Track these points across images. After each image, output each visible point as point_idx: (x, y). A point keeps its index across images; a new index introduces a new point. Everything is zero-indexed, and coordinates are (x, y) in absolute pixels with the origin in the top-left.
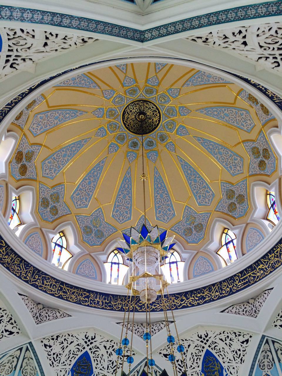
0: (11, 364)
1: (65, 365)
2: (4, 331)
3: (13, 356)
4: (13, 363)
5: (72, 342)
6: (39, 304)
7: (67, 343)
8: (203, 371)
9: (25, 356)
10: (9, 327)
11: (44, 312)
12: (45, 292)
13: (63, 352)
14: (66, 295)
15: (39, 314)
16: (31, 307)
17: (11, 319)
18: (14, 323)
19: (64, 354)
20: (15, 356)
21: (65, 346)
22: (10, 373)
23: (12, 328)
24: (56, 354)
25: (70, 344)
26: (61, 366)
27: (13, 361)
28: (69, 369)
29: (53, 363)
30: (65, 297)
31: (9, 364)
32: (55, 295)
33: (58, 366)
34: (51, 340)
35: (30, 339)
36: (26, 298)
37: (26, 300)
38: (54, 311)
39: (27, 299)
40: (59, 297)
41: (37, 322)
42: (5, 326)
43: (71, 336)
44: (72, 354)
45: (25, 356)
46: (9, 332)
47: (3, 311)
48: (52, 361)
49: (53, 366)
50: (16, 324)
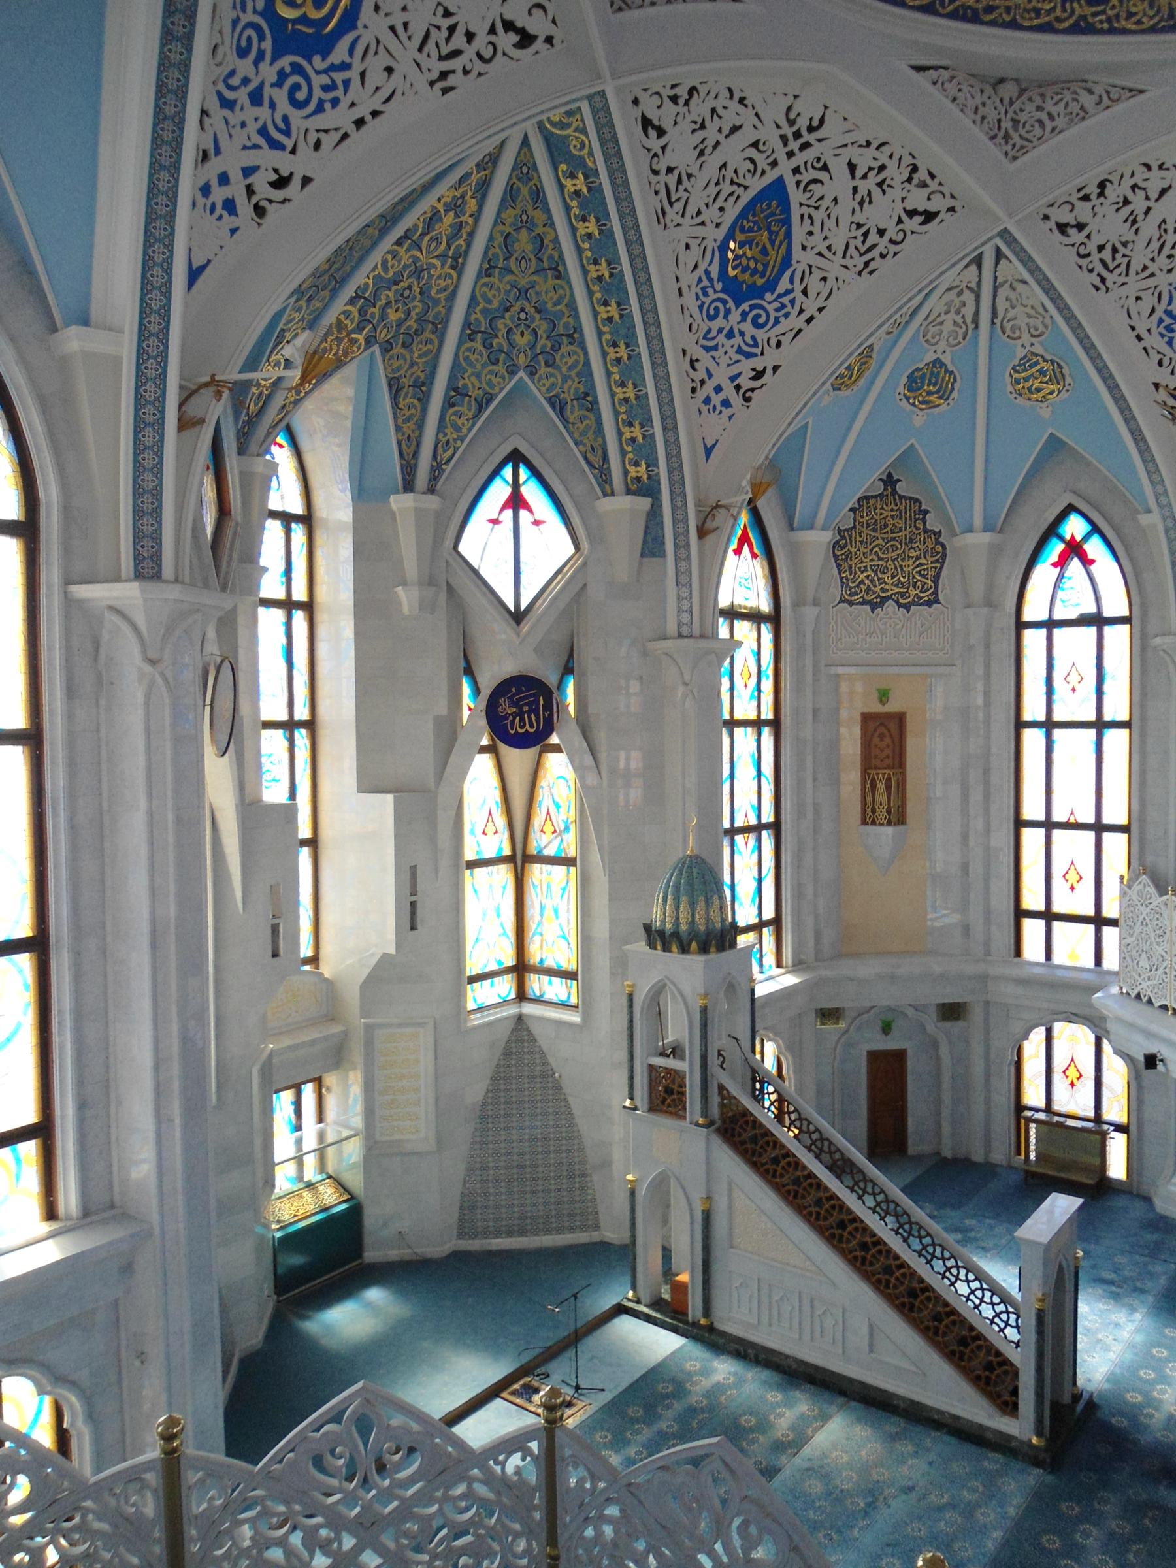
1: (1153, 275)
2: (905, 217)
4: (963, 310)
5: (1163, 192)
6: (1002, 81)
7: (1147, 198)
10: (918, 199)
11: (1030, 107)
12: (1014, 25)
13: (1137, 232)
14: (1104, 12)
15: (1012, 120)
16: (971, 103)
17: (915, 169)
18: (929, 181)
20: (963, 285)
22: (964, 339)
23: (929, 199)
25: (1157, 200)
30: (1101, 22)
31: (952, 315)
32: (1057, 25)
34: (1079, 205)
36: (946, 74)
37: (947, 85)
38: (1065, 92)
39: (952, 78)
40: (1075, 29)
41: (1011, 154)
42: (903, 199)
43: (1155, 167)
46: (920, 214)
47: (877, 148)
50: (937, 181)
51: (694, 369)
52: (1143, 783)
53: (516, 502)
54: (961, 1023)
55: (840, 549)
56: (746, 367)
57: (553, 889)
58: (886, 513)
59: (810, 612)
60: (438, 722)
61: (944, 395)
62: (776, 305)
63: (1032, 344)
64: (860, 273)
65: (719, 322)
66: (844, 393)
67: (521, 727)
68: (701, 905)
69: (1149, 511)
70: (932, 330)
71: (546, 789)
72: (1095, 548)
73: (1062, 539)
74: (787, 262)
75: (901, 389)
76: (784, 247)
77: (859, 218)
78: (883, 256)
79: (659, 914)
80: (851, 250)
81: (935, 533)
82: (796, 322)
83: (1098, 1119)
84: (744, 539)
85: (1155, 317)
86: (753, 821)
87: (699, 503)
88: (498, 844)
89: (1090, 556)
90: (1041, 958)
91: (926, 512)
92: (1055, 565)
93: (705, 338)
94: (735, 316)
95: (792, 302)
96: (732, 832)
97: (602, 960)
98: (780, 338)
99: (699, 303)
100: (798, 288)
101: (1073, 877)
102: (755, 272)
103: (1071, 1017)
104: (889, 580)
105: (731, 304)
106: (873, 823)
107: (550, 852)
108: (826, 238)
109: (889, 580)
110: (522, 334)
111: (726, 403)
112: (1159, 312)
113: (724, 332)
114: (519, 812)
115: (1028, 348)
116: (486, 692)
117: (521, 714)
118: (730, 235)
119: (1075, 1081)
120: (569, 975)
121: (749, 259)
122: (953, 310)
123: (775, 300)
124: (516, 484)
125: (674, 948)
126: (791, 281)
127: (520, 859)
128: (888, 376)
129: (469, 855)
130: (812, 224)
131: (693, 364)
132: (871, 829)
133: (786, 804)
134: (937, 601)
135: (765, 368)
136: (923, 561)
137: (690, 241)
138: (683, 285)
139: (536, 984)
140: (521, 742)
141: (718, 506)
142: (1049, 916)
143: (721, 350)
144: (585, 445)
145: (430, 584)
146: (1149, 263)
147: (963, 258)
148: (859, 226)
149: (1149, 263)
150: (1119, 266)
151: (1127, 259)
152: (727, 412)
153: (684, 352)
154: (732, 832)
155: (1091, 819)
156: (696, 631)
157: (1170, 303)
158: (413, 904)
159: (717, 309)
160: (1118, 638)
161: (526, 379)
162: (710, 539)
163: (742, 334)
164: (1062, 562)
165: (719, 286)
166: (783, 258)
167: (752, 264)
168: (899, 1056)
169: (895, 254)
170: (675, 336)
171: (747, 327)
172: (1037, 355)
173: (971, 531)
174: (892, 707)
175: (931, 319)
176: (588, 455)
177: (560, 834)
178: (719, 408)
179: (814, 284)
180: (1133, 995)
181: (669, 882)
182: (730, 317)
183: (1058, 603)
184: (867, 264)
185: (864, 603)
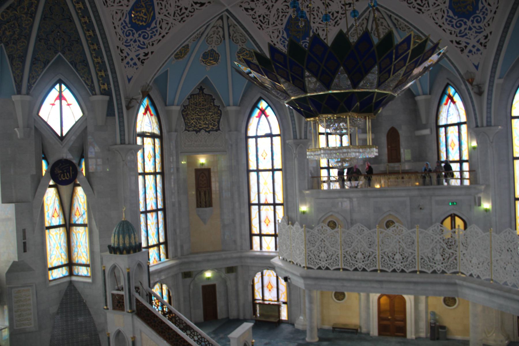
1: (277, 25)
4: (219, 34)
7: (272, 2)
8: (450, 7)
9: (228, 24)
19: (272, 14)
21: (270, 6)
24: (262, 16)
27: (219, 32)
31: (216, 35)
35: (224, 6)
44: (280, 12)
45: (228, 24)
46: (199, 3)
53: (61, 97)
55: (185, 112)
56: (141, 52)
57: (81, 236)
59: (174, 134)
61: (216, 60)
62: (151, 32)
64: (180, 22)
68: (127, 238)
70: (209, 40)
71: (77, 200)
73: (259, 108)
74: (154, 18)
75: (201, 59)
76: (152, 13)
77: (178, 4)
78: (187, 16)
79: (113, 241)
80: (176, 14)
81: (217, 106)
84: (147, 109)
86: (154, 208)
87: (126, 98)
88: (58, 220)
89: (268, 114)
90: (259, 249)
92: (257, 117)
93: (126, 42)
94: (136, 35)
95: (157, 31)
96: (146, 212)
100: (158, 26)
101: (267, 221)
102: (142, 21)
104: (202, 123)
105: (134, 31)
106: (201, 207)
108: (167, 10)
109: (202, 123)
110: (59, 40)
114: (67, 208)
116: (51, 165)
117: (63, 173)
118: (133, 9)
121: (140, 17)
123: (151, 30)
124: (61, 92)
126: (156, 24)
127: (68, 226)
129: (47, 224)
130: (162, 6)
133: (167, 202)
134: (219, 130)
135: (148, 53)
137: (118, 11)
138: (116, 25)
140: (65, 183)
142: (261, 235)
143: (132, 47)
144: (84, 78)
145: (28, 127)
146: (275, 22)
147: (217, 16)
148: (178, 7)
149: (275, 22)
151: (267, 21)
152: (135, 67)
153: (118, 47)
154: (146, 212)
155: (272, 202)
156: (132, 143)
157: (283, 34)
158: (25, 244)
159: (129, 33)
160: (277, 141)
161: (61, 54)
163: (139, 41)
164: (259, 116)
165: (129, 26)
166: (152, 16)
167: (141, 18)
169: (192, 16)
170: (114, 42)
171: (141, 39)
173: (229, 105)
175: (209, 36)
179: (164, 25)
183: (258, 129)
184: (182, 19)
185: (194, 130)
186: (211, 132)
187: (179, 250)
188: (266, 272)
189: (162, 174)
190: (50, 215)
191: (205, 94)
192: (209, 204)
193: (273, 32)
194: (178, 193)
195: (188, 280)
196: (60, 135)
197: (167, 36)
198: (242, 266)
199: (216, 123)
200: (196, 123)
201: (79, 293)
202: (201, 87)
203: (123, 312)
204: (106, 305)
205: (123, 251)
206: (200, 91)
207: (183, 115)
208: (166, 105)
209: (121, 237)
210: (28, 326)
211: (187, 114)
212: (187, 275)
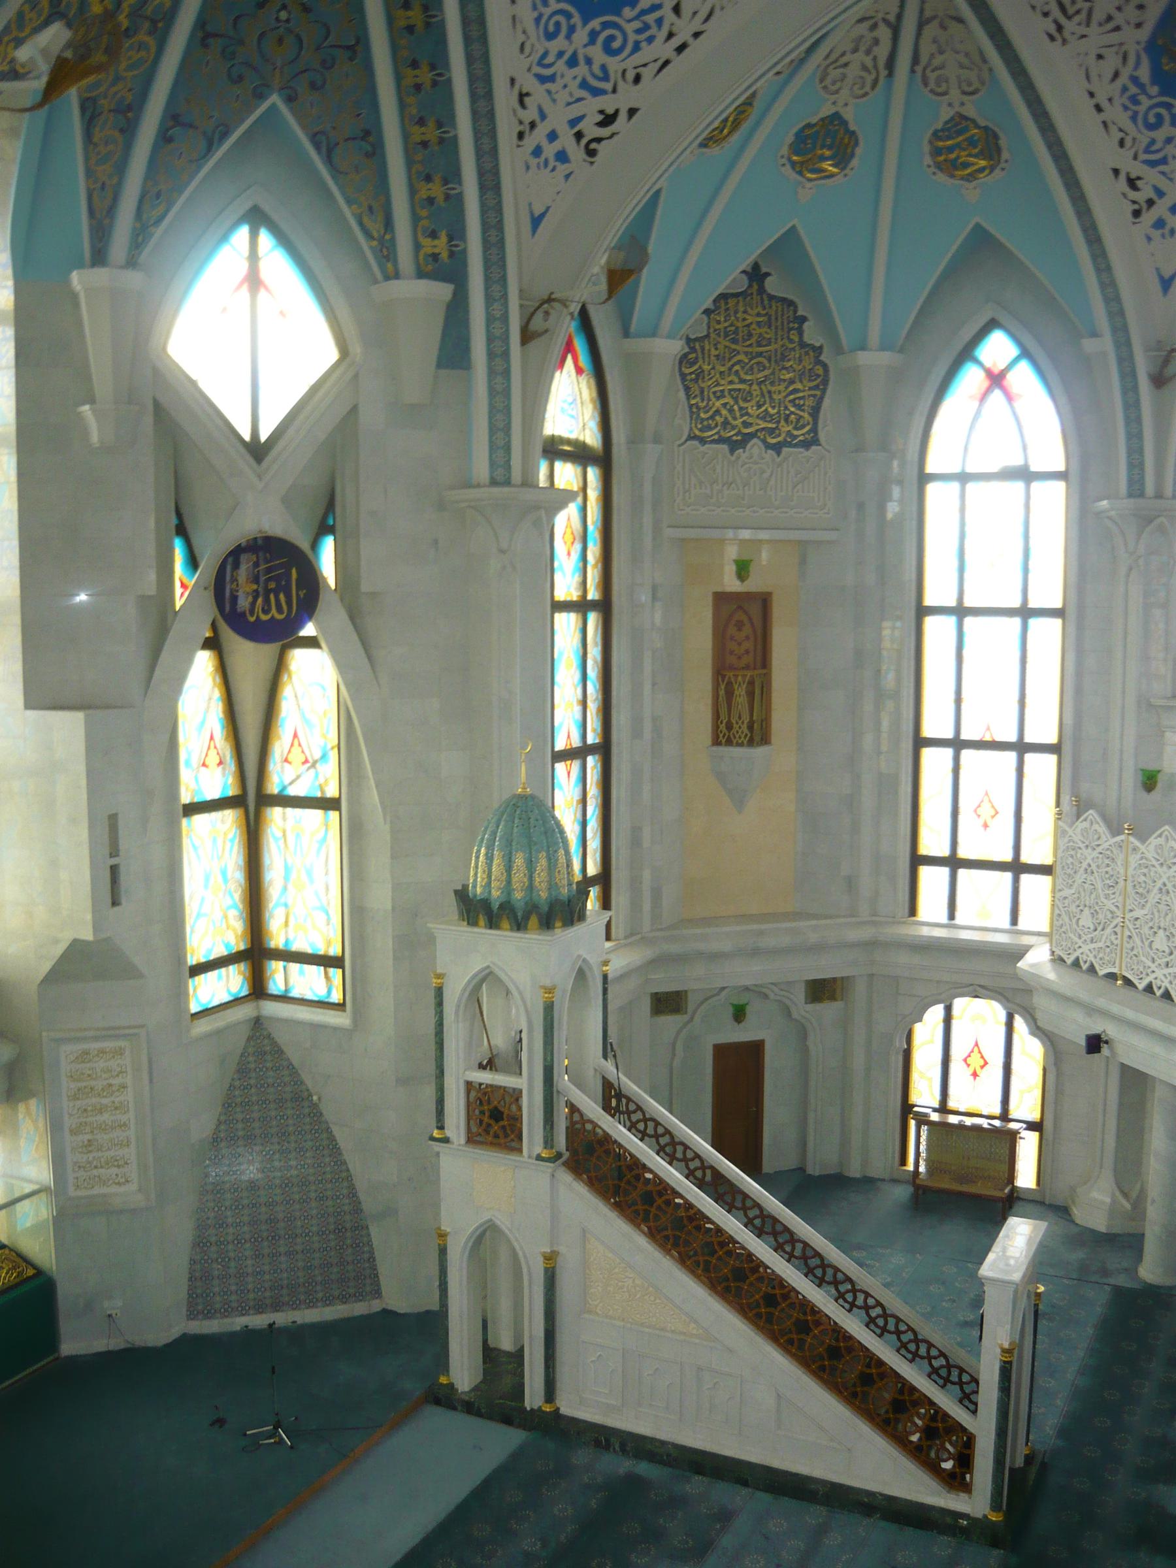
0: (868, 52)
1: (1117, 28)
3: (872, 17)
4: (875, 49)
22: (873, 87)
26: (1097, 37)
28: (1138, 43)
29: (1060, 28)
31: (860, 56)
33: (1084, 36)
45: (922, 11)
48: (1056, 22)
49: (1064, 42)
51: (522, 103)
52: (1079, 690)
54: (837, 1005)
58: (750, 319)
60: (143, 600)
61: (843, 159)
62: (637, 24)
63: (963, 104)
65: (559, 43)
66: (715, 151)
67: (265, 612)
69: (1094, 334)
70: (834, 73)
72: (1024, 378)
75: (785, 150)
81: (813, 348)
82: (661, 49)
83: (1005, 1116)
85: (1119, 83)
86: (576, 742)
91: (804, 319)
93: (540, 64)
94: (581, 36)
95: (660, 22)
97: (383, 942)
98: (639, 70)
99: (536, 14)
101: (986, 812)
103: (977, 991)
105: (577, 19)
106: (729, 742)
107: (297, 790)
111: (562, 156)
112: (1124, 79)
113: (566, 56)
114: (251, 732)
115: (957, 109)
116: (209, 560)
119: (978, 1071)
120: (326, 961)
122: (863, 48)
124: (253, 256)
125: (482, 922)
127: (252, 801)
128: (773, 130)
131: (522, 97)
132: (721, 748)
133: (620, 718)
135: (617, 111)
136: (798, 386)
139: (278, 976)
140: (256, 632)
141: (550, 300)
142: (954, 863)
143: (560, 82)
149: (1116, 14)
150: (1078, 12)
152: (562, 168)
155: (1013, 737)
158: (114, 870)
159: (558, 24)
162: (533, 345)
168: (755, 1049)
170: (506, 61)
171: (597, 52)
172: (966, 118)
173: (863, 348)
174: (753, 585)
176: (366, 220)
177: (314, 765)
178: (552, 163)
180: (1069, 962)
181: (494, 833)
182: (575, 36)
185: (721, 440)
186: (785, 450)
187: (647, 906)
188: (959, 1004)
189: (605, 606)
190: (195, 761)
191: (772, 298)
192: (759, 734)
193: (1100, 57)
194: (654, 684)
195: (670, 1022)
196: (247, 438)
197: (694, 44)
198: (878, 981)
199: (806, 415)
200: (731, 411)
201: (290, 1066)
202: (756, 266)
203: (513, 1157)
204: (441, 1128)
205: (527, 917)
206: (750, 286)
207: (683, 376)
208: (626, 334)
209: (519, 860)
210: (114, 1189)
211: (700, 375)
212: (667, 1003)
